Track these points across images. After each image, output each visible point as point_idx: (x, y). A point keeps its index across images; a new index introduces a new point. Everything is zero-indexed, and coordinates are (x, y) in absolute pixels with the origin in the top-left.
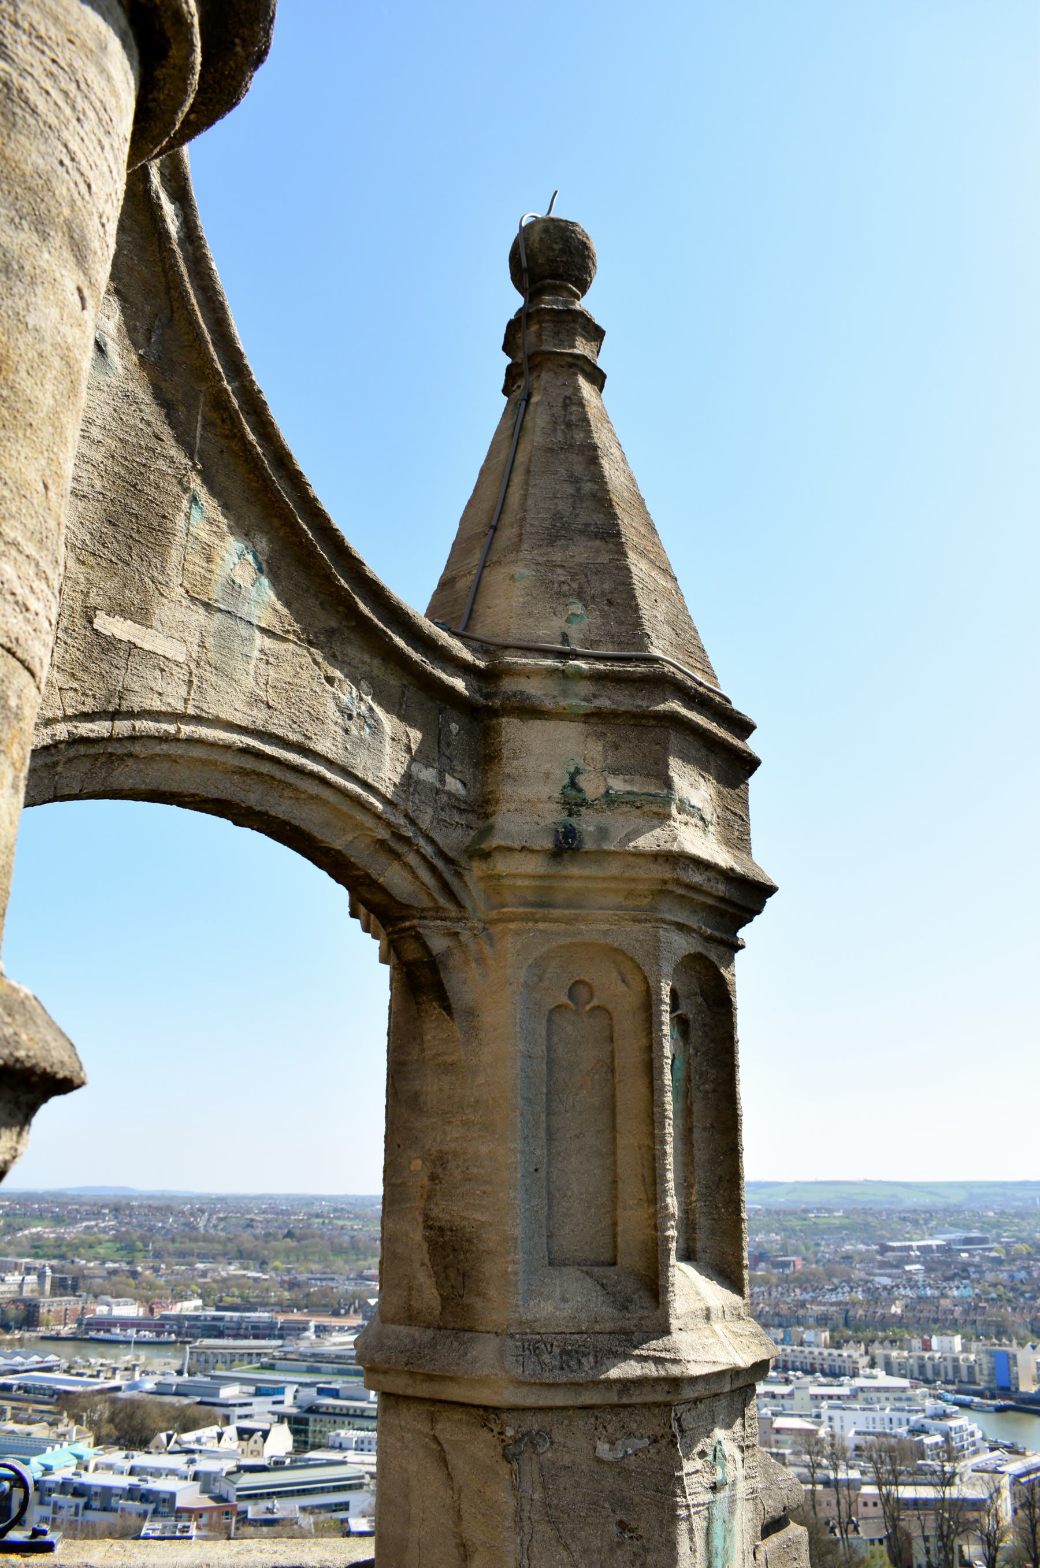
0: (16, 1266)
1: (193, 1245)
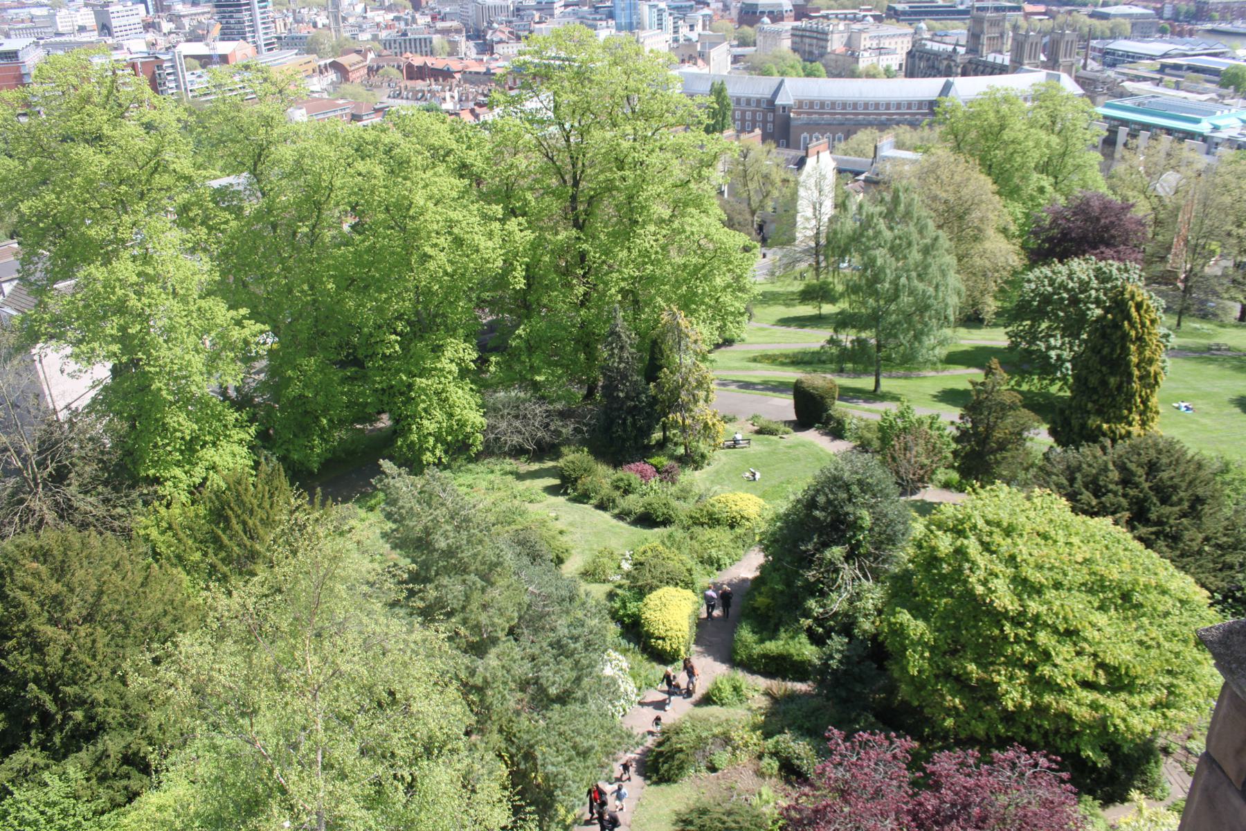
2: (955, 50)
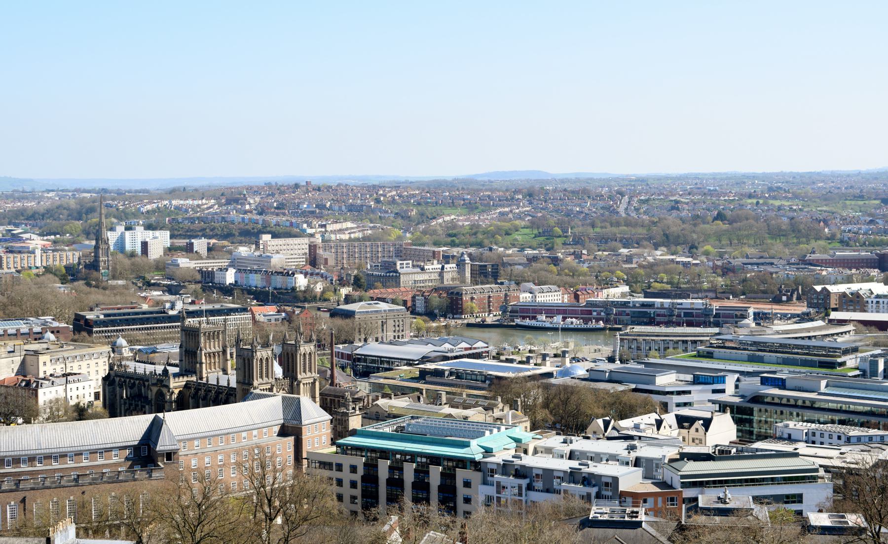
0: (434, 255)
1: (614, 229)
2: (165, 372)
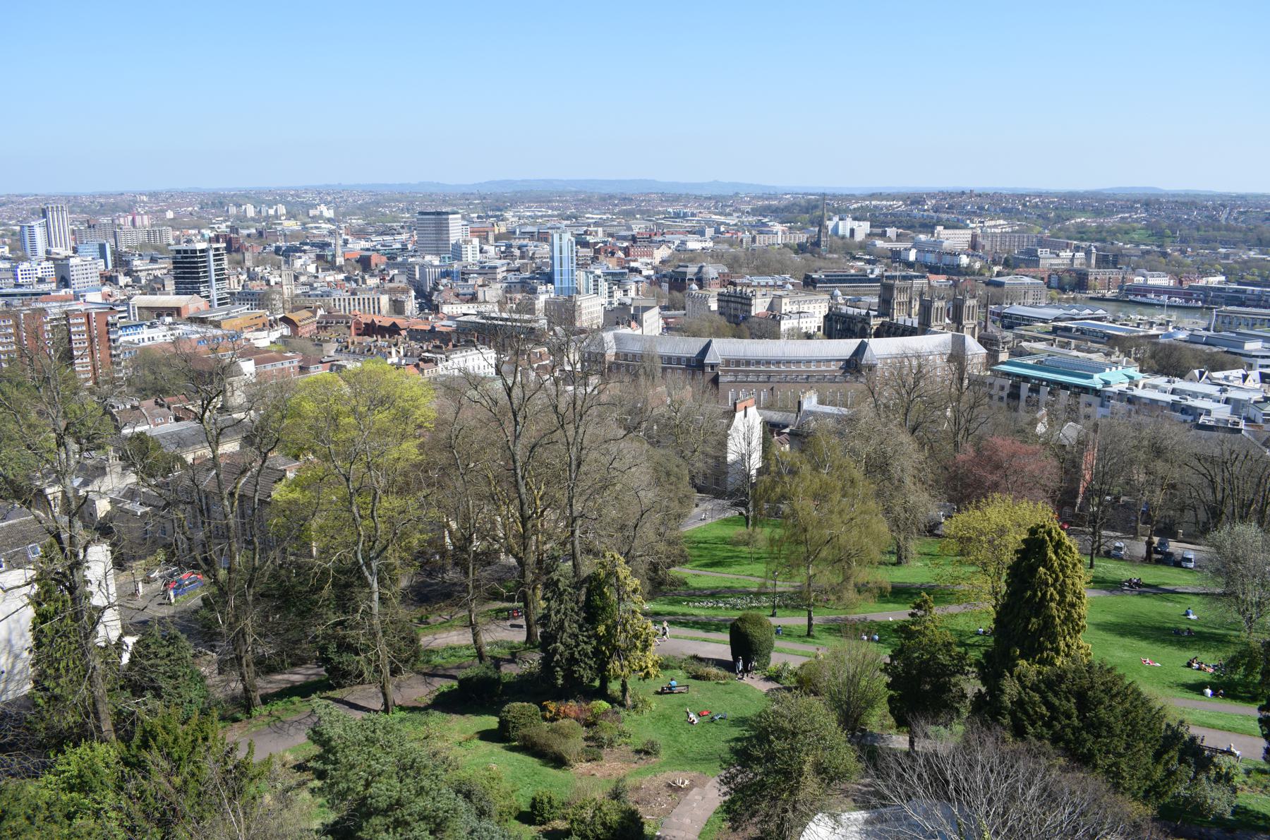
1: (1216, 233)
